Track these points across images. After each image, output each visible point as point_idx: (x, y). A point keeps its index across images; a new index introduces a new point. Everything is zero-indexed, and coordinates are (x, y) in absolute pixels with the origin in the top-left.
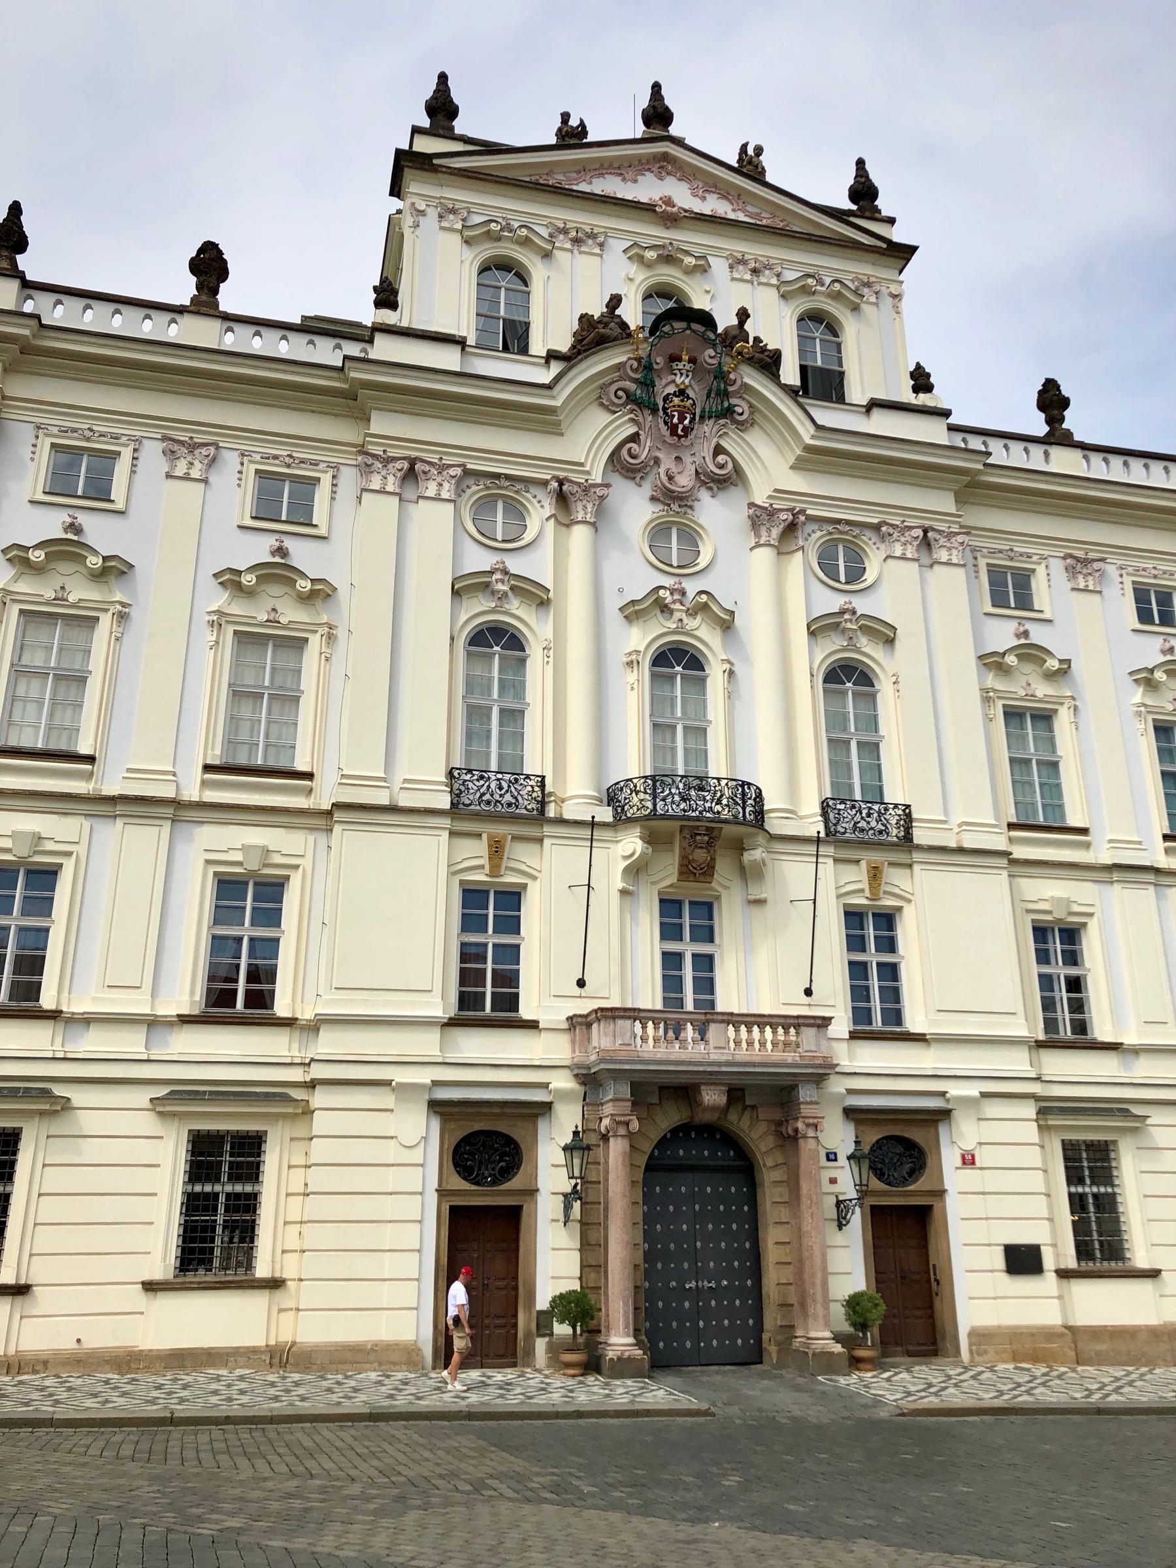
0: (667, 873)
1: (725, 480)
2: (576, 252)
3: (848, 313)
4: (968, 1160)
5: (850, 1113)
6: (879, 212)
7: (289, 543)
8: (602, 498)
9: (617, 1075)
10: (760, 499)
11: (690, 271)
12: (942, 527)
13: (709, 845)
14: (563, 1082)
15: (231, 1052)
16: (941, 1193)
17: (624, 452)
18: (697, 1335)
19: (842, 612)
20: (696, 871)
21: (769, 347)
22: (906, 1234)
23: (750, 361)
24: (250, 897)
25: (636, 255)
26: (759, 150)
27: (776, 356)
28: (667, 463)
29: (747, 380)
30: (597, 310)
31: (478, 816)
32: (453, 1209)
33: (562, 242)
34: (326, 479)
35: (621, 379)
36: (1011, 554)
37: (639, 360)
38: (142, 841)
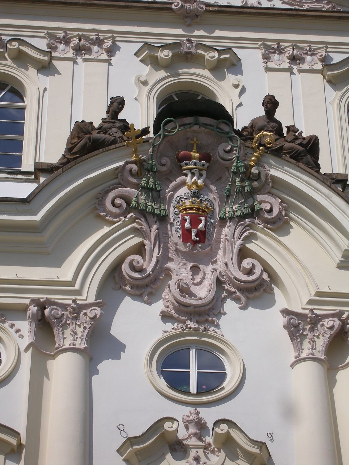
2: (79, 60)
17: (125, 268)
21: (304, 135)
23: (278, 152)
25: (149, 56)
28: (180, 270)
29: (273, 172)
30: (97, 116)
35: (120, 185)
37: (139, 163)
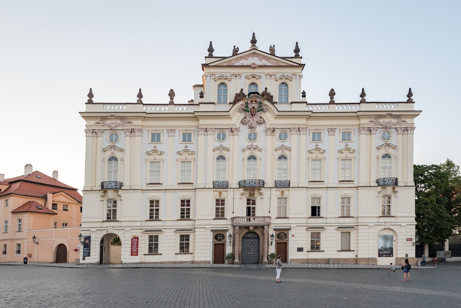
1: (261, 122)
4: (293, 236)
5: (274, 229)
7: (188, 145)
8: (239, 130)
12: (302, 127)
14: (230, 227)
15: (185, 224)
16: (288, 240)
18: (249, 260)
19: (282, 146)
20: (252, 195)
24: (185, 203)
30: (238, 92)
36: (317, 129)
38: (170, 195)
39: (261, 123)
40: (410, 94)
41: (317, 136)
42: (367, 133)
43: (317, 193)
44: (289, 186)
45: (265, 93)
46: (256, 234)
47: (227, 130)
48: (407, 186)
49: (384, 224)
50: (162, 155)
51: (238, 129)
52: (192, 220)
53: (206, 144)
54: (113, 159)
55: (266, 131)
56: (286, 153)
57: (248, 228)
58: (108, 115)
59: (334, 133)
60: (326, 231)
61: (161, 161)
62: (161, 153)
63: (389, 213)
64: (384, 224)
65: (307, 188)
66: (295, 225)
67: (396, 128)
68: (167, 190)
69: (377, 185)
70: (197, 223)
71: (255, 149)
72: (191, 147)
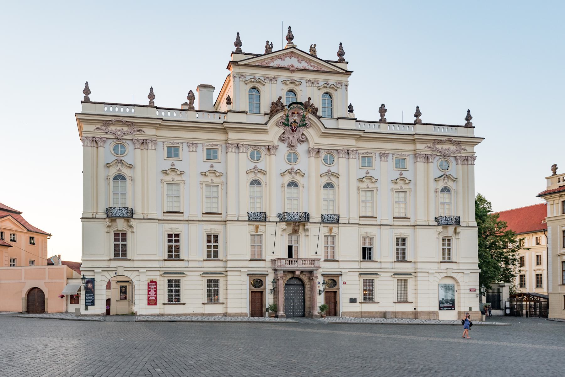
0: (290, 230)
3: (334, 92)
4: (345, 283)
5: (322, 275)
6: (344, 60)
9: (281, 270)
10: (312, 146)
11: (296, 85)
12: (352, 149)
13: (299, 226)
14: (271, 271)
16: (339, 289)
22: (332, 298)
24: (213, 239)
26: (315, 45)
27: (317, 109)
30: (275, 100)
31: (253, 221)
32: (252, 292)
33: (267, 81)
34: (220, 149)
38: (193, 227)
39: (302, 142)
40: (469, 117)
41: (367, 161)
42: (424, 160)
43: (370, 231)
44: (338, 222)
45: (307, 104)
46: (300, 280)
47: (263, 148)
48: (469, 227)
49: (445, 271)
50: (182, 175)
51: (276, 148)
52: (222, 261)
53: (237, 164)
54: (120, 177)
55: (309, 152)
56: (334, 180)
57: (293, 272)
58: (113, 119)
59: (387, 158)
60: (380, 278)
61: (181, 184)
62: (182, 173)
63: (449, 258)
64: (445, 271)
65: (359, 224)
66: (346, 270)
67: (455, 157)
68: (190, 221)
69: (436, 223)
70: (229, 264)
71: (296, 173)
72: (218, 167)
